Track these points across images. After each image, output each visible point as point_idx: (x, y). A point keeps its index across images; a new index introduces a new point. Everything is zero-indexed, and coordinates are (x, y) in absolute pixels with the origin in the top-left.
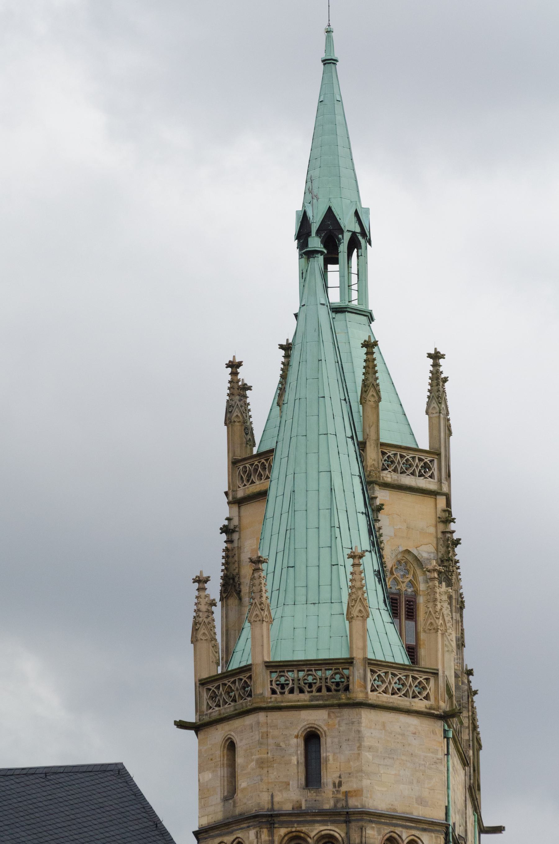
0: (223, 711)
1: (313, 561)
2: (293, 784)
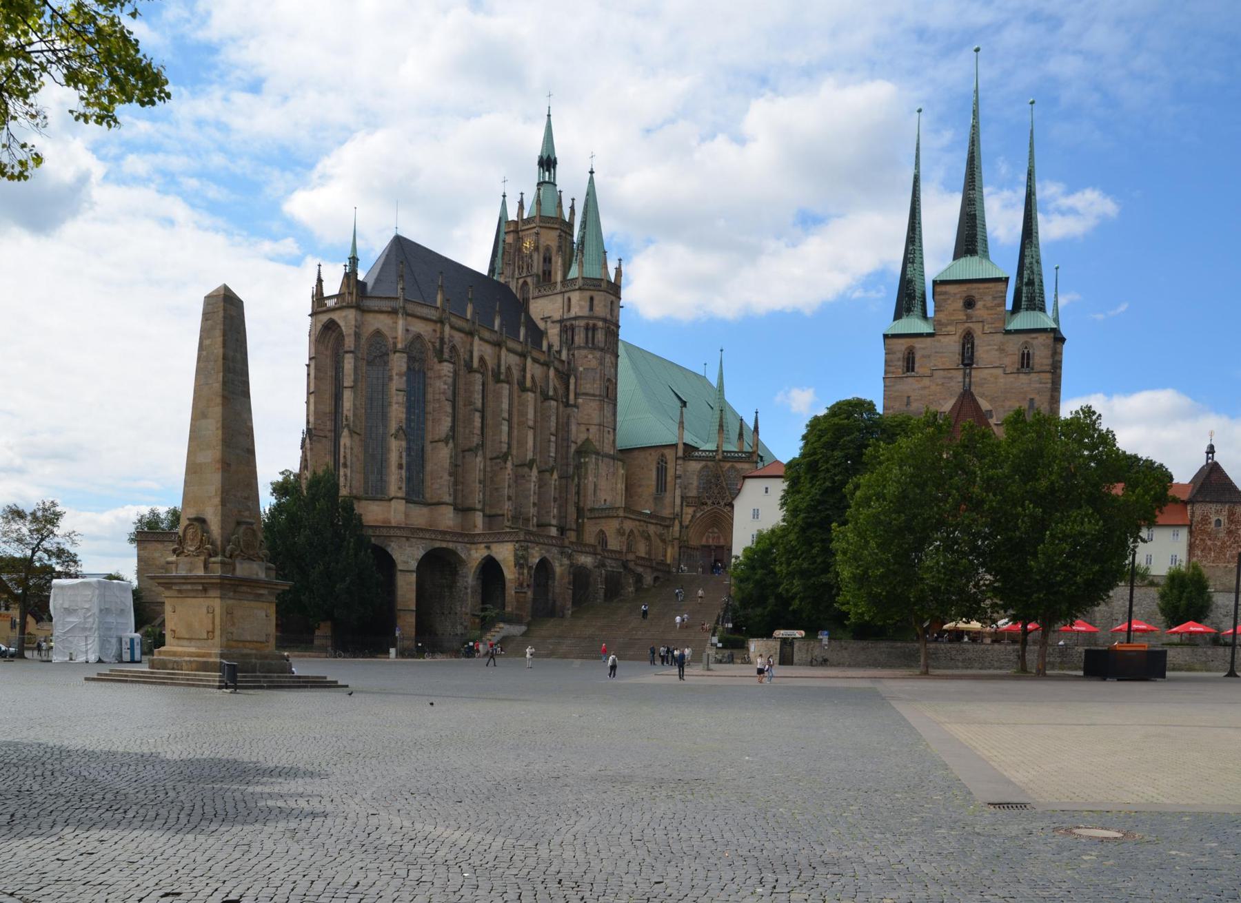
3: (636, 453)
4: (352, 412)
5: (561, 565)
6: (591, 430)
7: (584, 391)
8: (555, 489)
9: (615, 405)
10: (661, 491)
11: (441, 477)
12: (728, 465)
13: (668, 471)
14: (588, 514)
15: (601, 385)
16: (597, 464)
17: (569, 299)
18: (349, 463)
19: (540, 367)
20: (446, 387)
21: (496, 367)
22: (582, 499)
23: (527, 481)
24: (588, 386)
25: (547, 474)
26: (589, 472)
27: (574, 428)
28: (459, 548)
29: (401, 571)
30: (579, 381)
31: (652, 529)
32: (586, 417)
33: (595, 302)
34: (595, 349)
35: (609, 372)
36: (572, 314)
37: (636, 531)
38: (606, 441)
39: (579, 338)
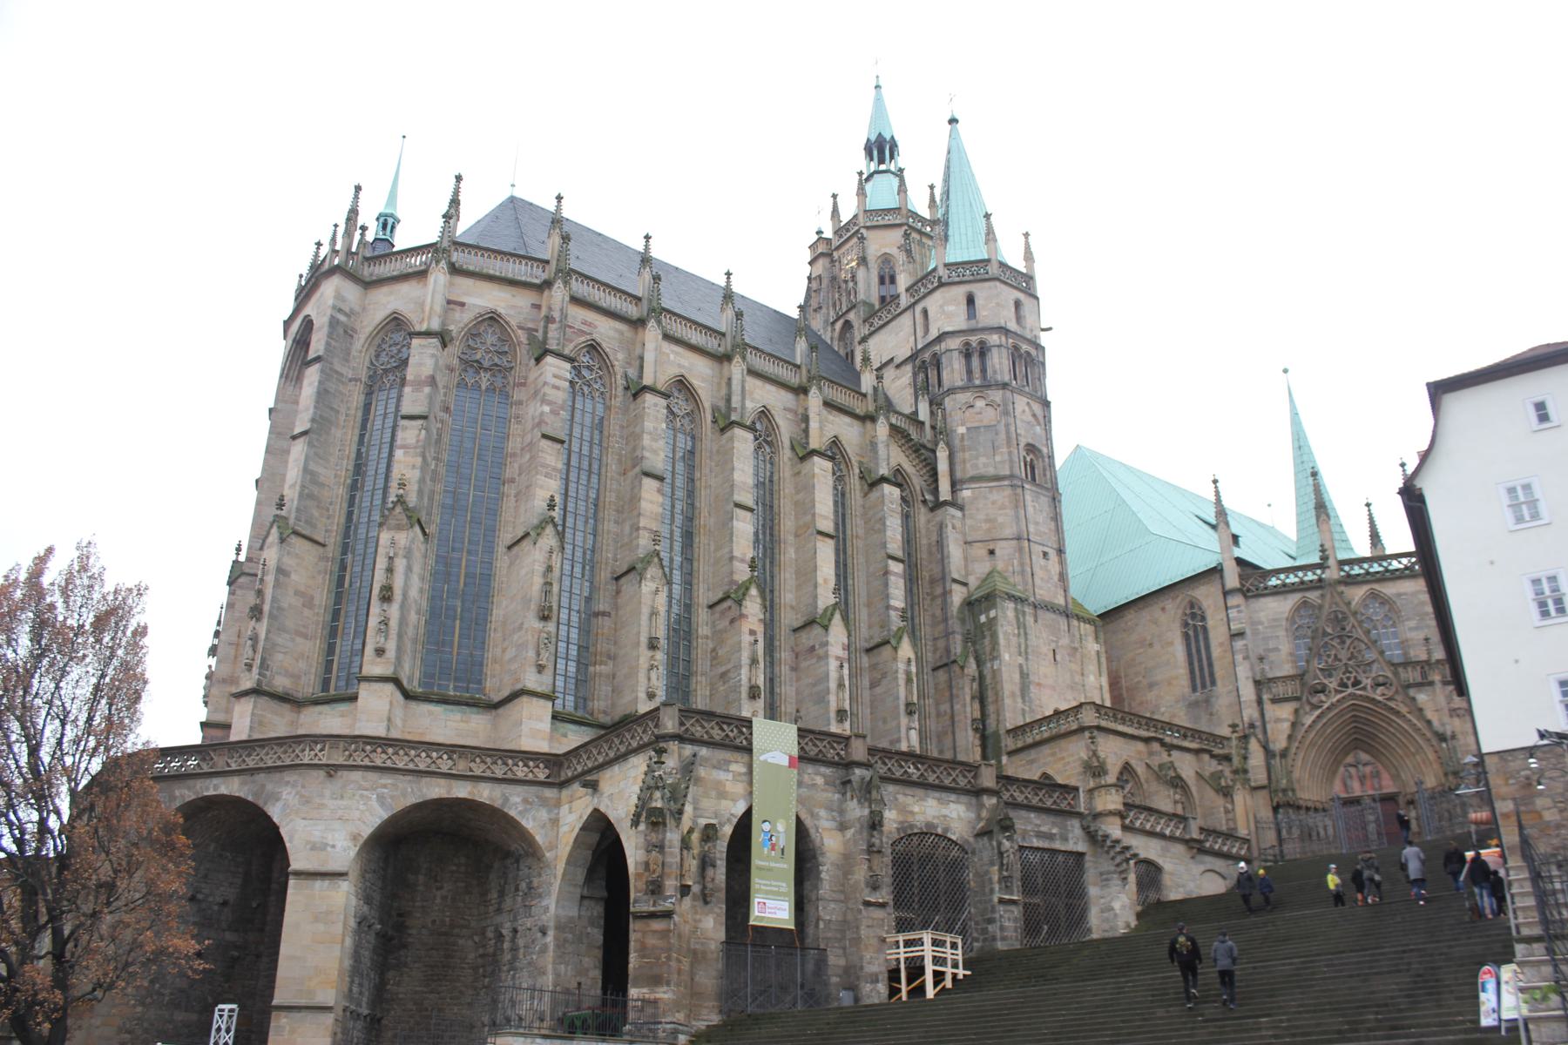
3: (1130, 616)
4: (298, 488)
5: (842, 827)
6: (998, 552)
7: (971, 473)
8: (909, 680)
9: (1055, 499)
10: (1204, 686)
11: (520, 627)
12: (1357, 594)
13: (1212, 635)
14: (1009, 743)
15: (1010, 453)
16: (1021, 625)
17: (925, 312)
18: (266, 608)
19: (856, 423)
20: (547, 409)
21: (722, 404)
22: (991, 709)
23: (820, 658)
24: (983, 460)
25: (886, 652)
26: (1002, 641)
27: (955, 552)
28: (516, 799)
29: (299, 874)
30: (959, 456)
31: (1186, 766)
32: (985, 526)
33: (979, 302)
34: (989, 386)
35: (1035, 434)
36: (934, 334)
37: (1140, 770)
38: (1039, 573)
39: (953, 371)
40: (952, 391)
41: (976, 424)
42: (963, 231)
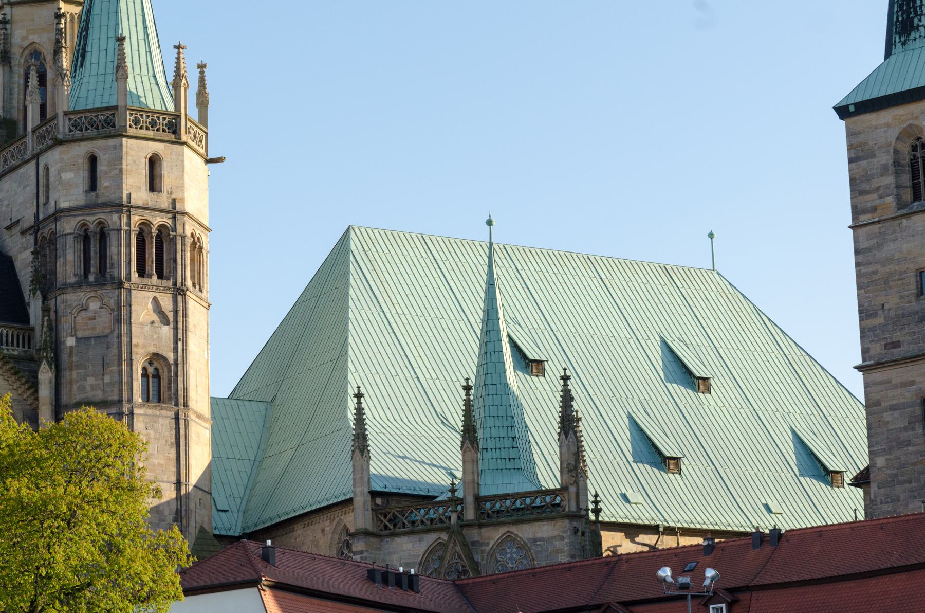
0: (87, 134)
1: (103, 47)
2: (143, 188)
7: (78, 397)
12: (494, 535)
24: (91, 381)
30: (66, 375)
33: (102, 167)
40: (65, 287)
41: (87, 334)
42: (103, 47)
